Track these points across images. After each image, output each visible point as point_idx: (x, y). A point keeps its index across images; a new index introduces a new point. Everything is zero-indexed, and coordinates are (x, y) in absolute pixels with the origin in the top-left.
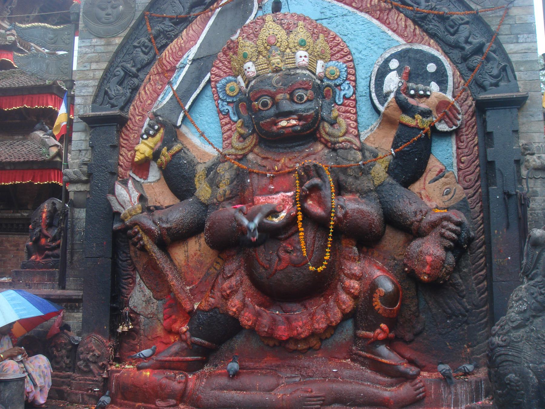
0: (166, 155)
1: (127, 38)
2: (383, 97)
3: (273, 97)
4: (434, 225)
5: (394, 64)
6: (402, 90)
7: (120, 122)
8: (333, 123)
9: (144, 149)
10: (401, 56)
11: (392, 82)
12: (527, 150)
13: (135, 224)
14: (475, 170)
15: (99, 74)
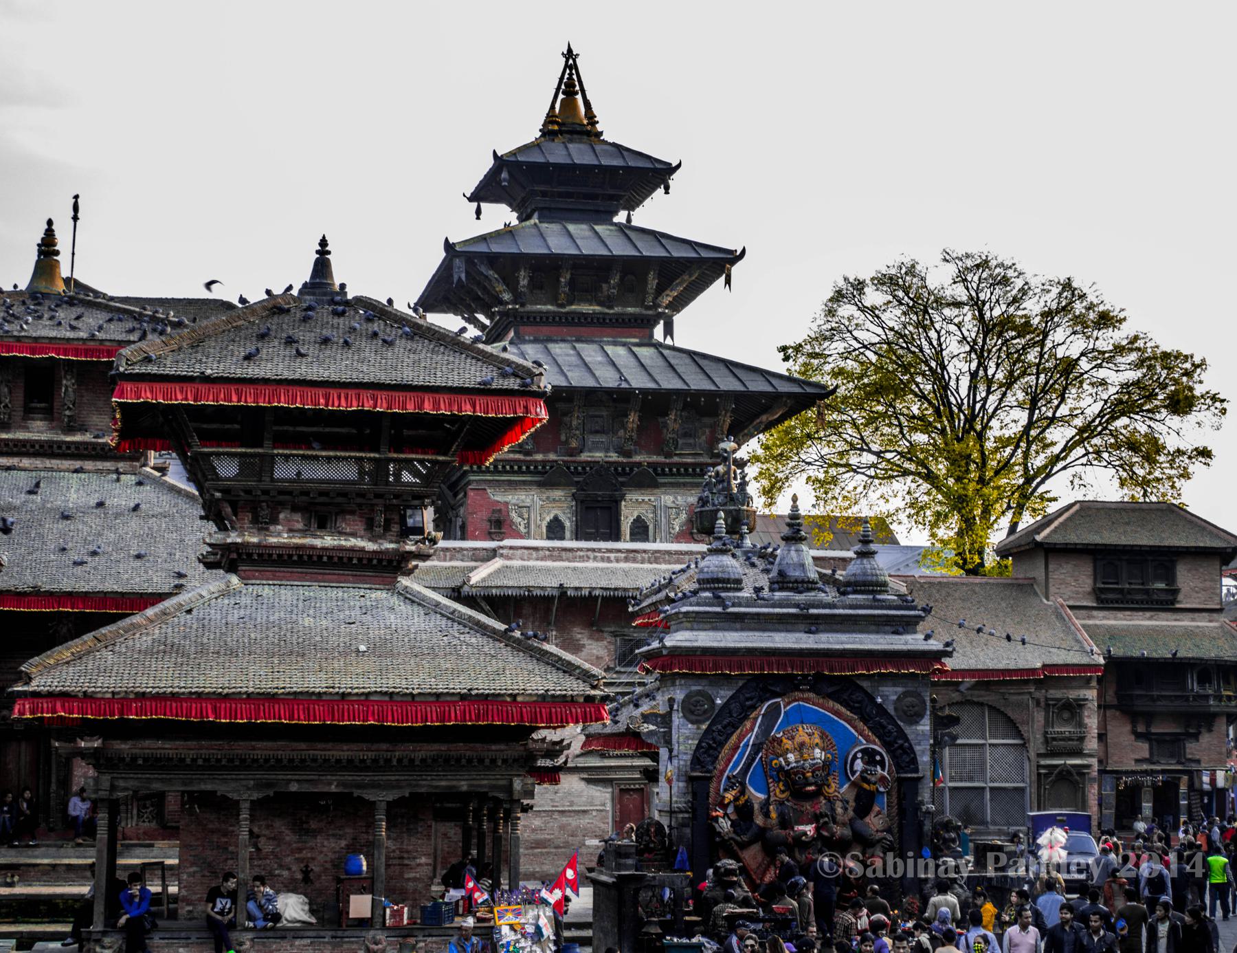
0: (742, 801)
1: (710, 726)
2: (853, 773)
3: (804, 774)
4: (879, 841)
5: (859, 755)
6: (862, 772)
7: (711, 778)
8: (829, 786)
9: (729, 796)
10: (864, 751)
11: (859, 765)
12: (922, 803)
13: (732, 839)
14: (895, 810)
15: (694, 748)
